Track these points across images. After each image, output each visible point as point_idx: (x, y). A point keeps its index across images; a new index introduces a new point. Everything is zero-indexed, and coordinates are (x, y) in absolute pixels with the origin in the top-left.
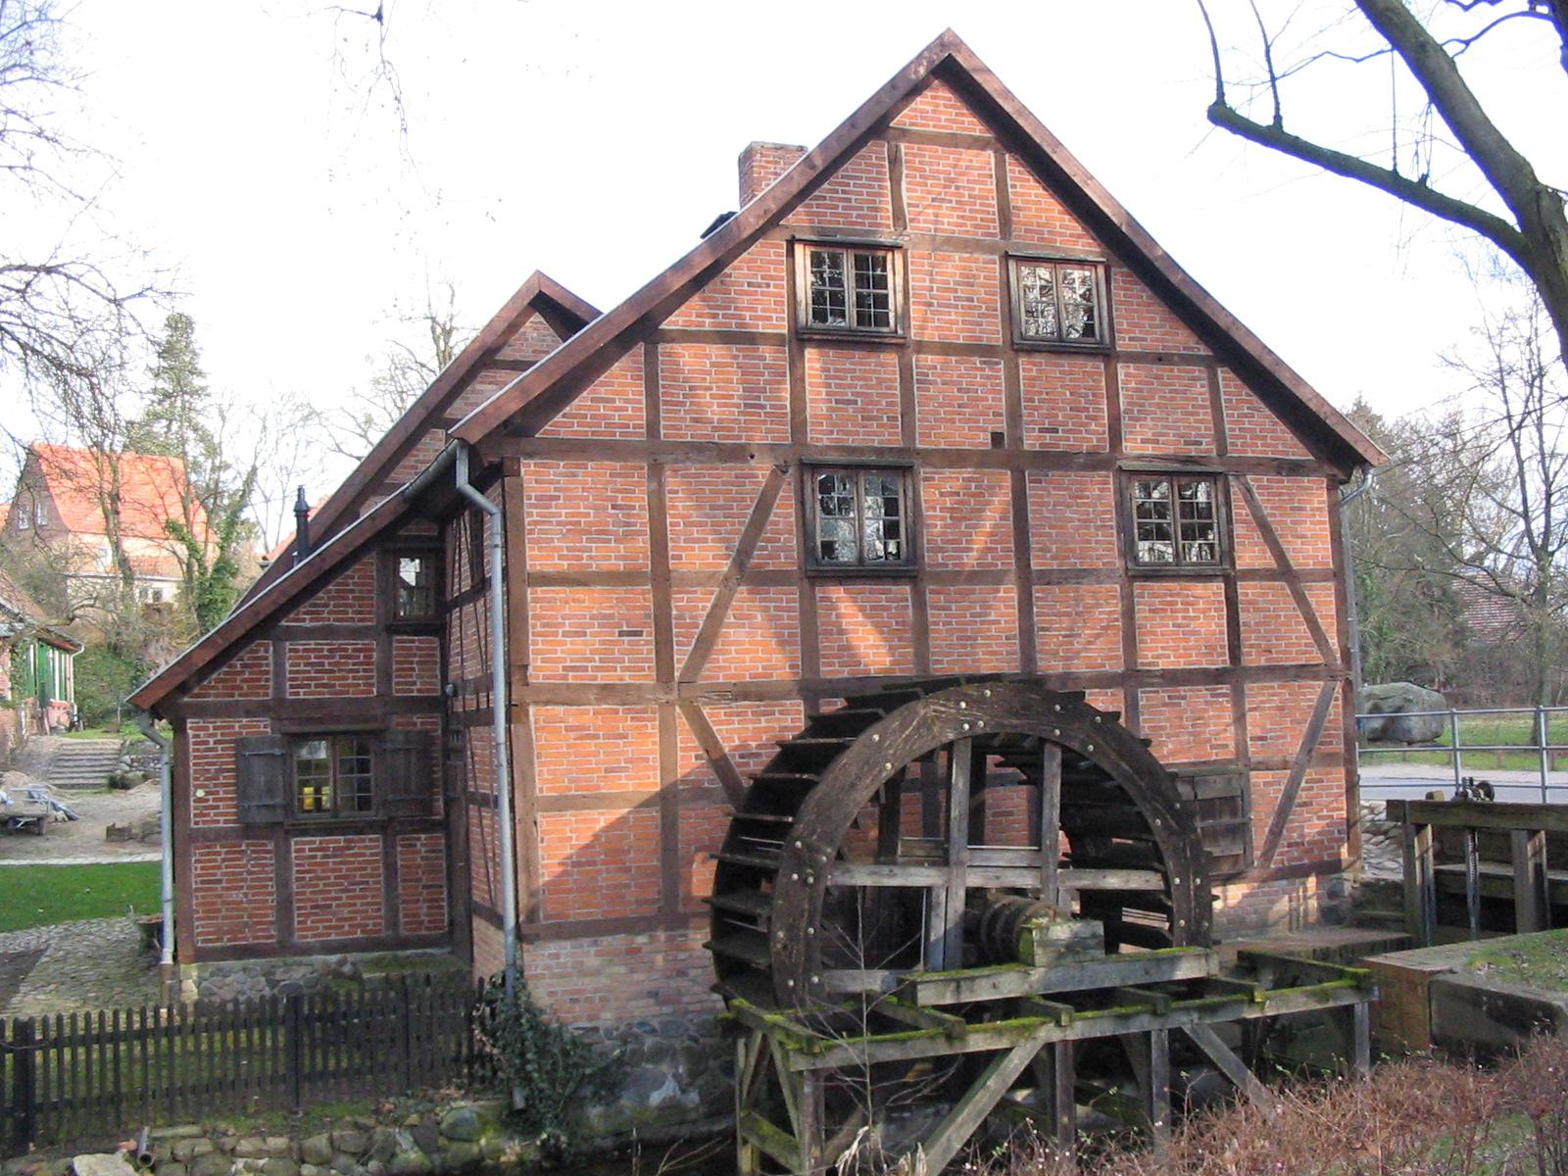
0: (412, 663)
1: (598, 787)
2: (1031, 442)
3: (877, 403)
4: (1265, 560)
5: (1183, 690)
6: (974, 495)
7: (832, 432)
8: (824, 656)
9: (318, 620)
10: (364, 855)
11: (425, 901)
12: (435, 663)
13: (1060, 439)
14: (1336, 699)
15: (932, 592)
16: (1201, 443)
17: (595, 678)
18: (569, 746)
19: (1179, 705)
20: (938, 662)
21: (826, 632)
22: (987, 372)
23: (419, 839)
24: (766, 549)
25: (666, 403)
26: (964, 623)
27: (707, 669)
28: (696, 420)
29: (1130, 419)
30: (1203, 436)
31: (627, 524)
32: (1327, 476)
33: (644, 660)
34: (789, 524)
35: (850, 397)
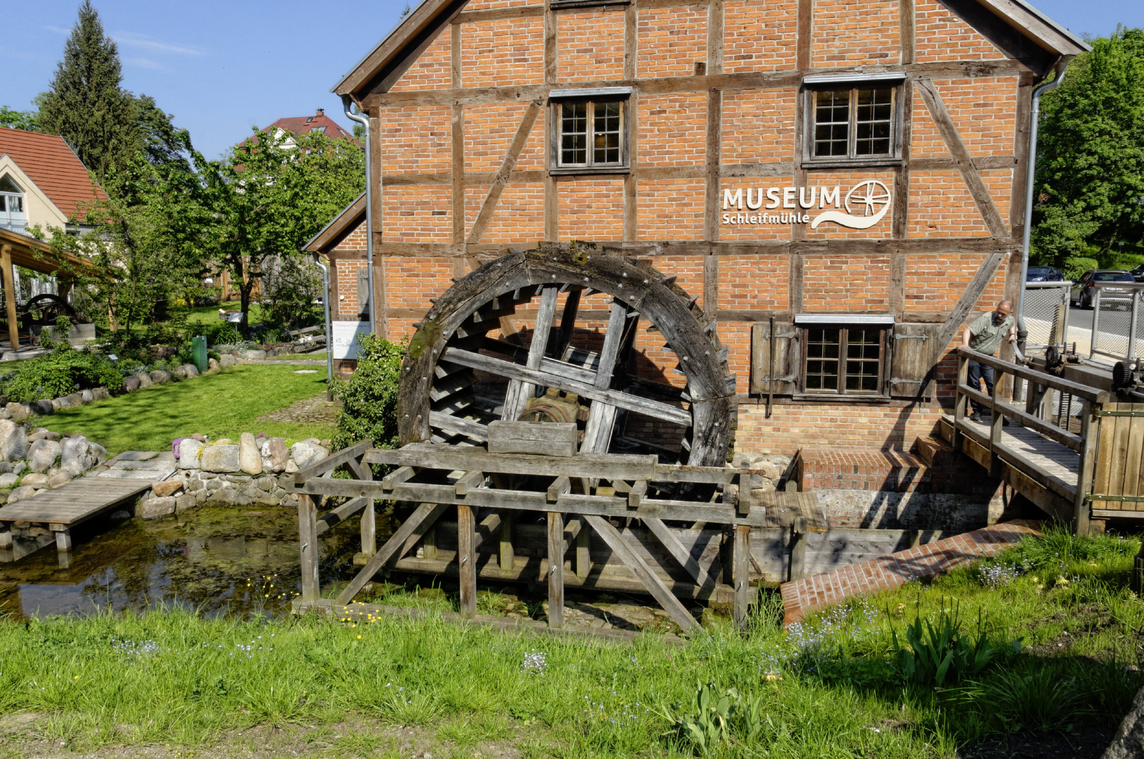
1: (419, 305)
2: (728, 68)
5: (844, 257)
6: (679, 112)
7: (573, 74)
8: (560, 228)
14: (1001, 268)
15: (641, 184)
16: (887, 55)
18: (404, 281)
19: (841, 268)
20: (641, 233)
24: (524, 157)
25: (465, 64)
26: (664, 206)
28: (483, 74)
29: (818, 41)
30: (889, 49)
31: (440, 145)
32: (1021, 73)
33: (447, 230)
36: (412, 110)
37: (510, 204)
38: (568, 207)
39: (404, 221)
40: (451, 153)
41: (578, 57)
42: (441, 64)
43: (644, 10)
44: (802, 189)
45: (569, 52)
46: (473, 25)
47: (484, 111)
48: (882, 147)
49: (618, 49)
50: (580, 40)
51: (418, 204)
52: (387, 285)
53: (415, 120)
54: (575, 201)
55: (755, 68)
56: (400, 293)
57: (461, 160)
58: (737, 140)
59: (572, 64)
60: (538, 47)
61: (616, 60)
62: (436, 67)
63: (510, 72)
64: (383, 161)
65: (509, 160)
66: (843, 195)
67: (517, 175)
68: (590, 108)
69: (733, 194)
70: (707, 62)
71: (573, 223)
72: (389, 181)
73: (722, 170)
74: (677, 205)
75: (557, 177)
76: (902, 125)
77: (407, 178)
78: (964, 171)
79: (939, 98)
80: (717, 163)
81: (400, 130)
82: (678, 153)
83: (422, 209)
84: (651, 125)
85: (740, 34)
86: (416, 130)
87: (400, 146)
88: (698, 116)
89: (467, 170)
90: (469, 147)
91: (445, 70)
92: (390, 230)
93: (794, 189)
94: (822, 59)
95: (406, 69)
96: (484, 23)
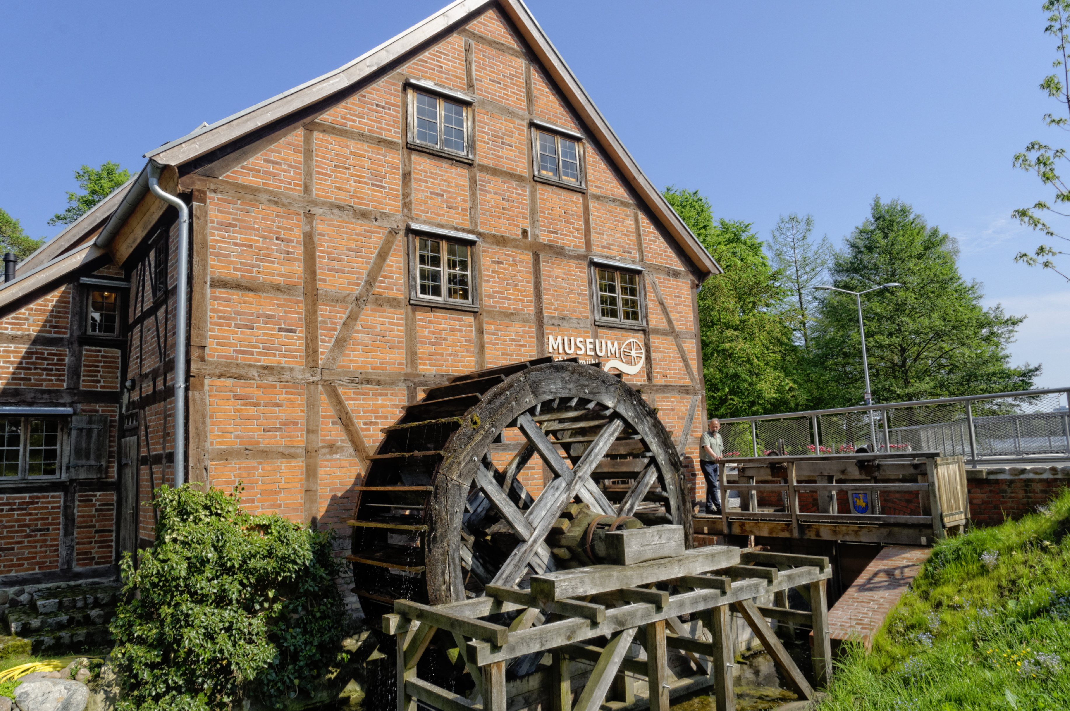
0: (98, 366)
1: (258, 443)
2: (544, 238)
3: (455, 198)
4: (663, 325)
6: (512, 265)
8: (421, 359)
9: (18, 330)
10: (47, 508)
11: (96, 542)
12: (117, 368)
13: (559, 238)
15: (487, 323)
17: (259, 361)
18: (237, 411)
21: (422, 342)
22: (519, 191)
23: (95, 496)
24: (383, 282)
25: (319, 173)
27: (342, 361)
28: (340, 189)
31: (288, 253)
33: (296, 351)
34: (399, 268)
35: (439, 191)
36: (252, 206)
37: (370, 329)
38: (425, 337)
39: (239, 335)
40: (302, 264)
41: (431, 198)
42: (290, 166)
43: (483, 174)
44: (597, 341)
45: (423, 191)
46: (328, 137)
47: (339, 226)
48: (635, 316)
49: (464, 201)
50: (433, 183)
51: (259, 316)
52: (211, 417)
53: (256, 218)
54: (433, 333)
55: (560, 243)
56: (230, 428)
57: (314, 273)
58: (553, 295)
59: (426, 203)
60: (395, 179)
61: (463, 209)
62: (284, 167)
63: (367, 194)
64: (210, 257)
65: (367, 282)
66: (620, 348)
67: (376, 299)
68: (444, 246)
69: (556, 339)
70: (529, 230)
71: (431, 354)
72: (219, 284)
73: (545, 320)
74: (516, 345)
75: (416, 306)
76: (643, 303)
77: (244, 282)
78: (675, 339)
79: (659, 288)
80: (541, 313)
81: (235, 226)
82: (514, 300)
83: (266, 323)
84: (493, 272)
85: (549, 214)
86: (257, 230)
87: (235, 244)
88: (526, 272)
89: (319, 285)
90: (322, 262)
91: (295, 173)
92: (218, 344)
93: (592, 340)
94: (598, 246)
95: (247, 159)
96: (338, 138)
